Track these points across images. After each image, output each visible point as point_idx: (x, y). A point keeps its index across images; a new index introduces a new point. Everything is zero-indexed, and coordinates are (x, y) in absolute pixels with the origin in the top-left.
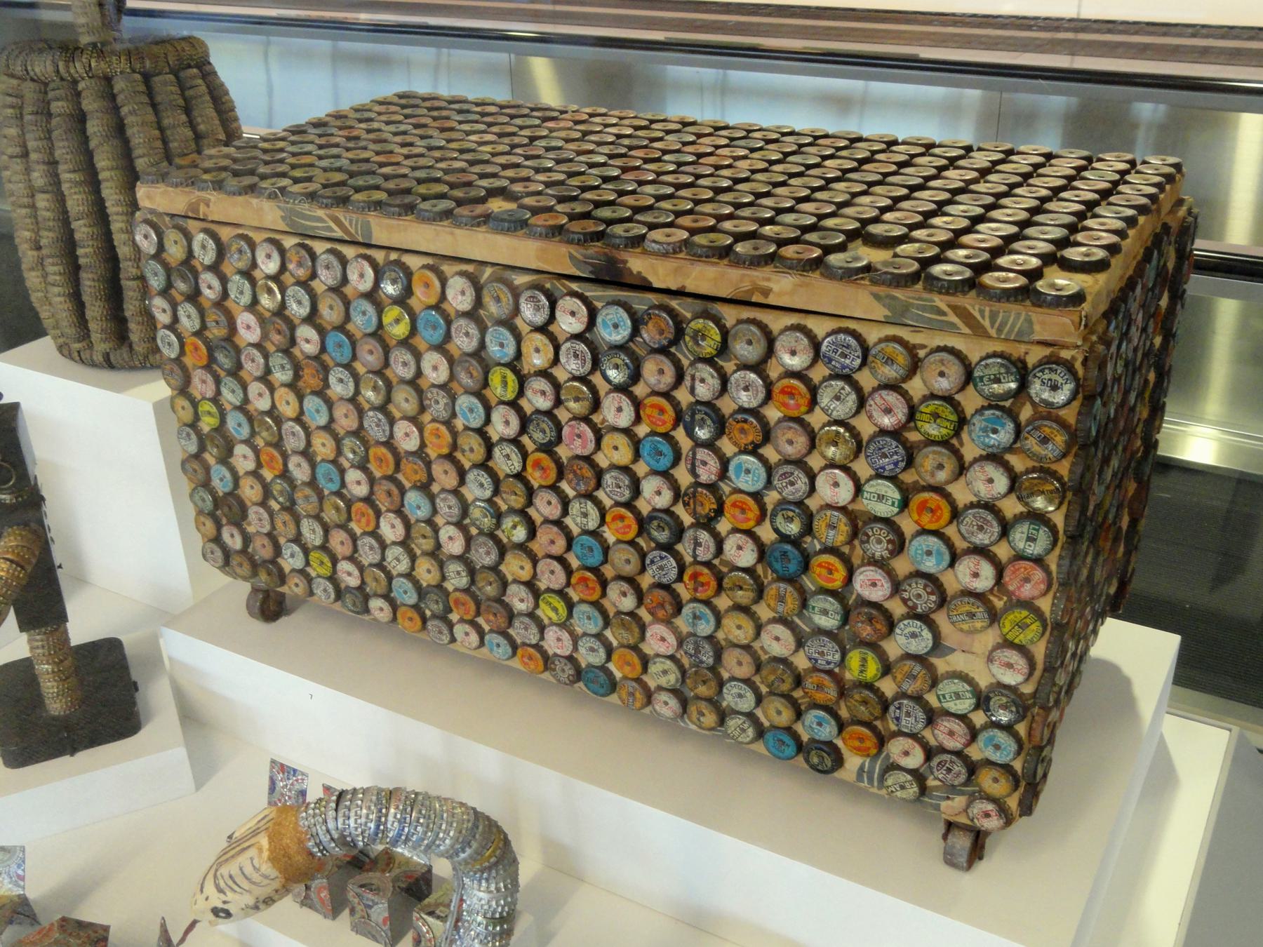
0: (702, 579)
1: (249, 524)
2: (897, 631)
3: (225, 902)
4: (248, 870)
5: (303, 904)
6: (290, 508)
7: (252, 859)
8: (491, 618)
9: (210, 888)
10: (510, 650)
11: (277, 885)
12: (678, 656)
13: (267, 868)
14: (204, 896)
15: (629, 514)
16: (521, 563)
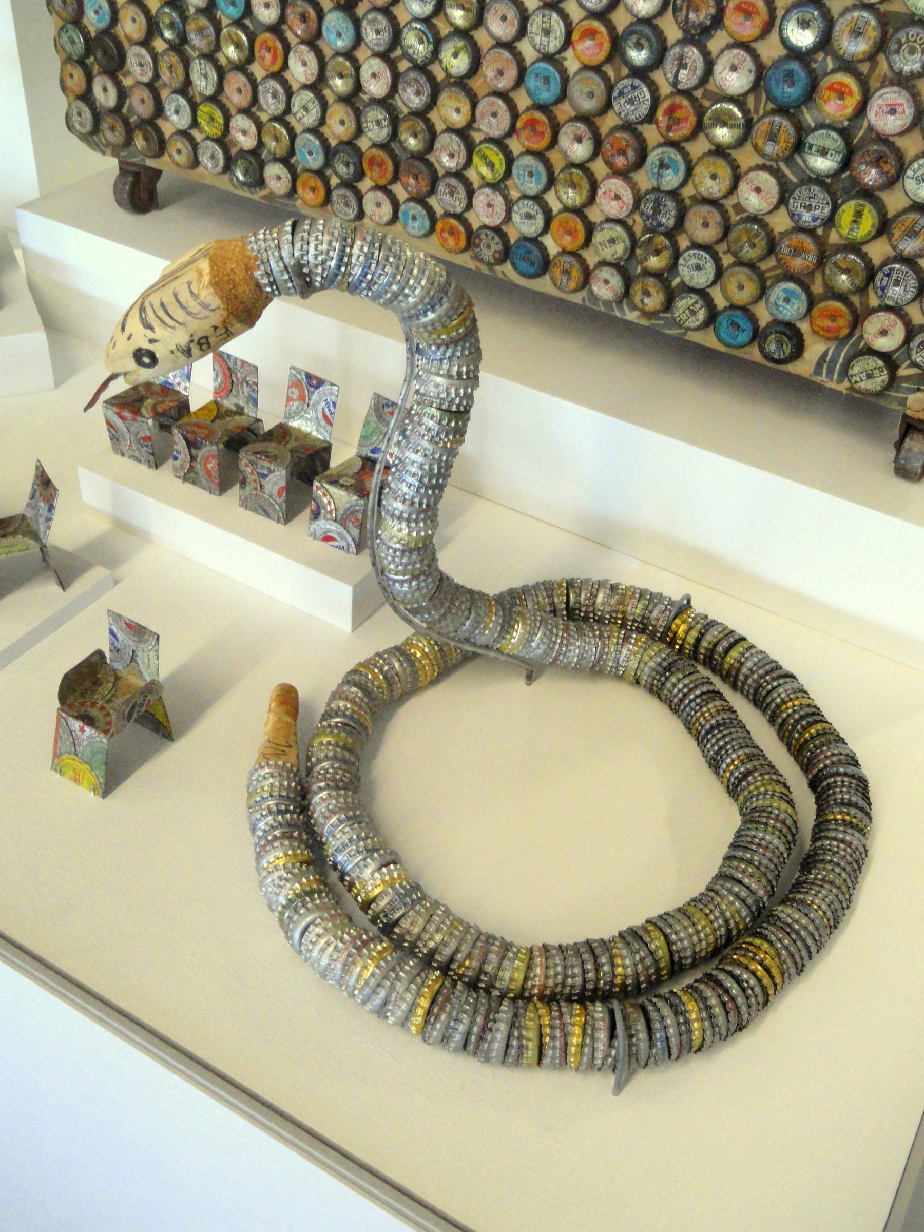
0: (678, 114)
1: (125, 75)
2: (909, 173)
3: (152, 341)
4: (185, 296)
5: (185, 479)
6: (179, 46)
7: (189, 284)
8: (412, 181)
9: (134, 325)
10: (427, 224)
11: (216, 319)
12: (630, 222)
13: (208, 295)
14: (126, 334)
15: (603, 29)
16: (457, 105)
